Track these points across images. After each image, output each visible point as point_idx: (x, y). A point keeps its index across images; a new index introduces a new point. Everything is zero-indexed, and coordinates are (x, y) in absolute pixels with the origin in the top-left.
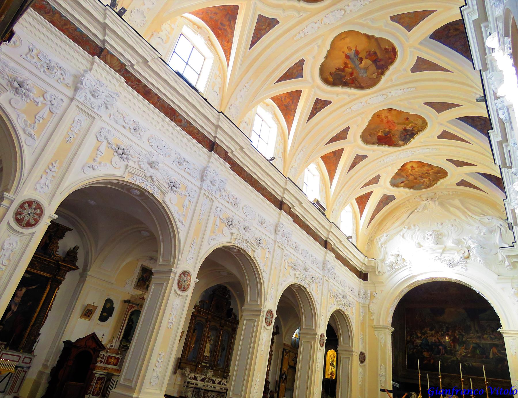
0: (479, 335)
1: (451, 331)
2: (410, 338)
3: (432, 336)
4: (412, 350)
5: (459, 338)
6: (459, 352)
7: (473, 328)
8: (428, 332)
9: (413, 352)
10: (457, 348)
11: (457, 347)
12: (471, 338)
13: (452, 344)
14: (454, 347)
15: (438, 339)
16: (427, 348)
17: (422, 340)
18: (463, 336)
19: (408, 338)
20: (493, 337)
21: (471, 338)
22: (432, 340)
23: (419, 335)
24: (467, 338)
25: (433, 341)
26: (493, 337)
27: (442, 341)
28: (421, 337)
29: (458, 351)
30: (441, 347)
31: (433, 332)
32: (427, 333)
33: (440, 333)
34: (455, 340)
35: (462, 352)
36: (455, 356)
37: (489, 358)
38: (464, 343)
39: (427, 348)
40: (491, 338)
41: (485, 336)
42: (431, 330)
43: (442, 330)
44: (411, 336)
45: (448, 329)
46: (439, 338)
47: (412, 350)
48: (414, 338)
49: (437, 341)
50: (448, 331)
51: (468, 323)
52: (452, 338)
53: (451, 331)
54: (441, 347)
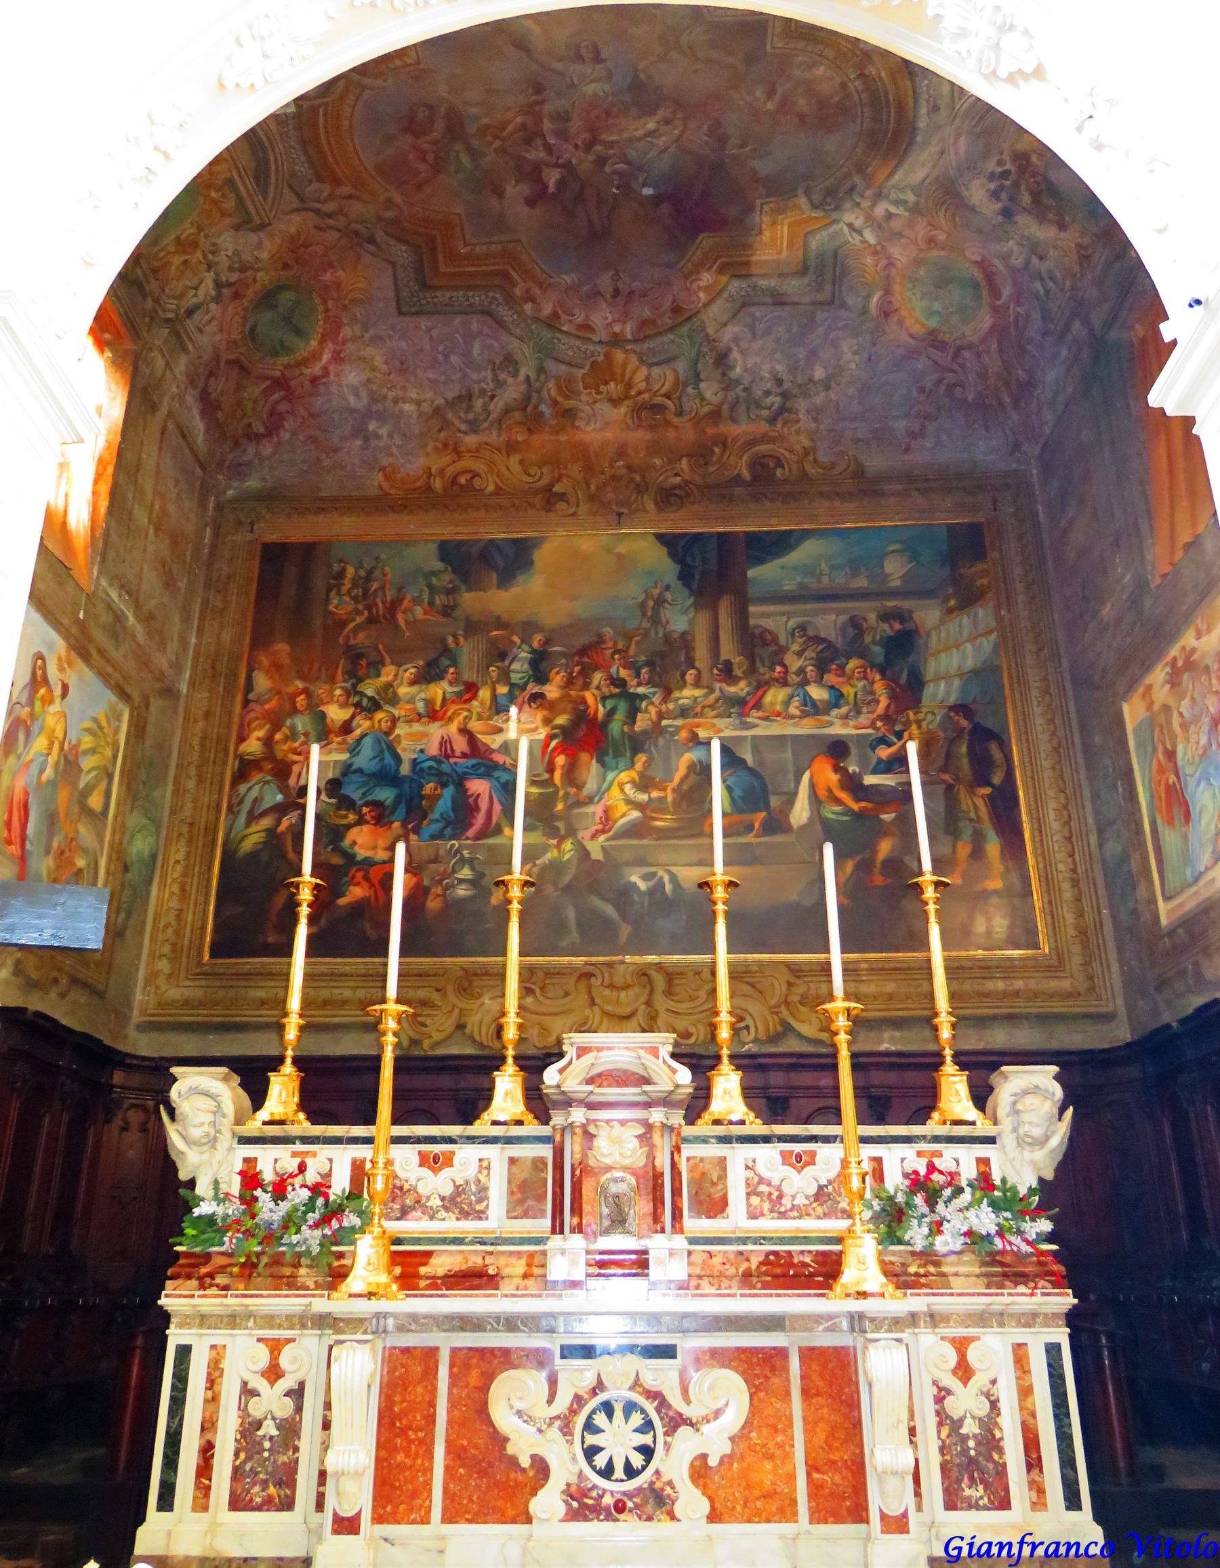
0: (740, 689)
1: (558, 678)
2: (268, 742)
3: (433, 714)
4: (266, 822)
5: (611, 714)
6: (596, 810)
7: (701, 654)
8: (403, 691)
9: (271, 832)
10: (591, 786)
11: (591, 772)
12: (684, 712)
13: (561, 760)
14: (571, 774)
15: (464, 731)
16: (386, 795)
17: (354, 750)
18: (634, 704)
19: (253, 746)
20: (817, 693)
21: (684, 712)
22: (418, 740)
23: (336, 714)
24: (661, 716)
25: (434, 750)
26: (817, 693)
27: (495, 742)
28: (347, 728)
29: (590, 800)
30: (478, 786)
31: (439, 690)
32: (394, 700)
33: (484, 694)
34: (583, 737)
35: (623, 807)
36: (572, 832)
37: (786, 828)
38: (636, 744)
39: (386, 795)
40: (807, 701)
41: (775, 696)
42: (428, 675)
43: (505, 676)
44: (276, 727)
45: (539, 669)
46: (475, 725)
47: (266, 822)
48: (293, 735)
49: (460, 745)
50: (542, 679)
51: (678, 623)
52: (561, 720)
53: (558, 678)
54: (478, 786)
